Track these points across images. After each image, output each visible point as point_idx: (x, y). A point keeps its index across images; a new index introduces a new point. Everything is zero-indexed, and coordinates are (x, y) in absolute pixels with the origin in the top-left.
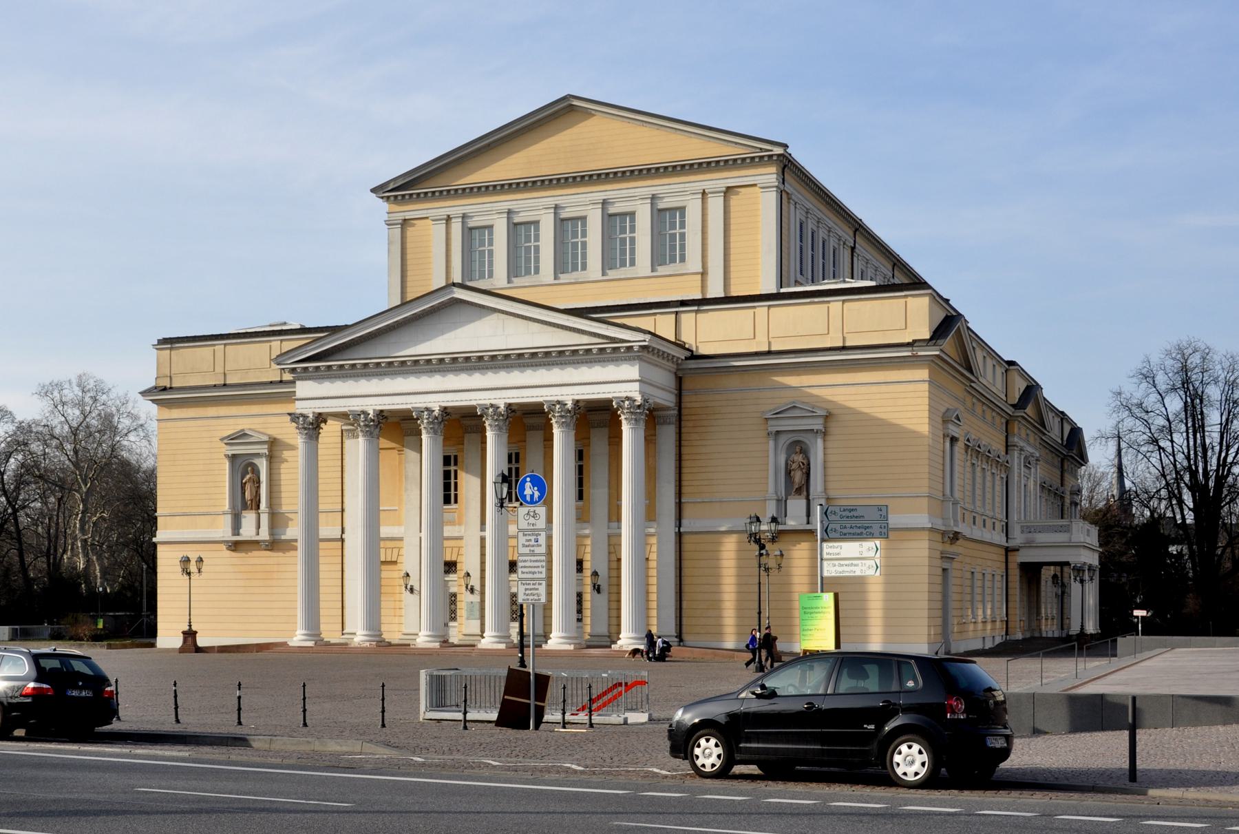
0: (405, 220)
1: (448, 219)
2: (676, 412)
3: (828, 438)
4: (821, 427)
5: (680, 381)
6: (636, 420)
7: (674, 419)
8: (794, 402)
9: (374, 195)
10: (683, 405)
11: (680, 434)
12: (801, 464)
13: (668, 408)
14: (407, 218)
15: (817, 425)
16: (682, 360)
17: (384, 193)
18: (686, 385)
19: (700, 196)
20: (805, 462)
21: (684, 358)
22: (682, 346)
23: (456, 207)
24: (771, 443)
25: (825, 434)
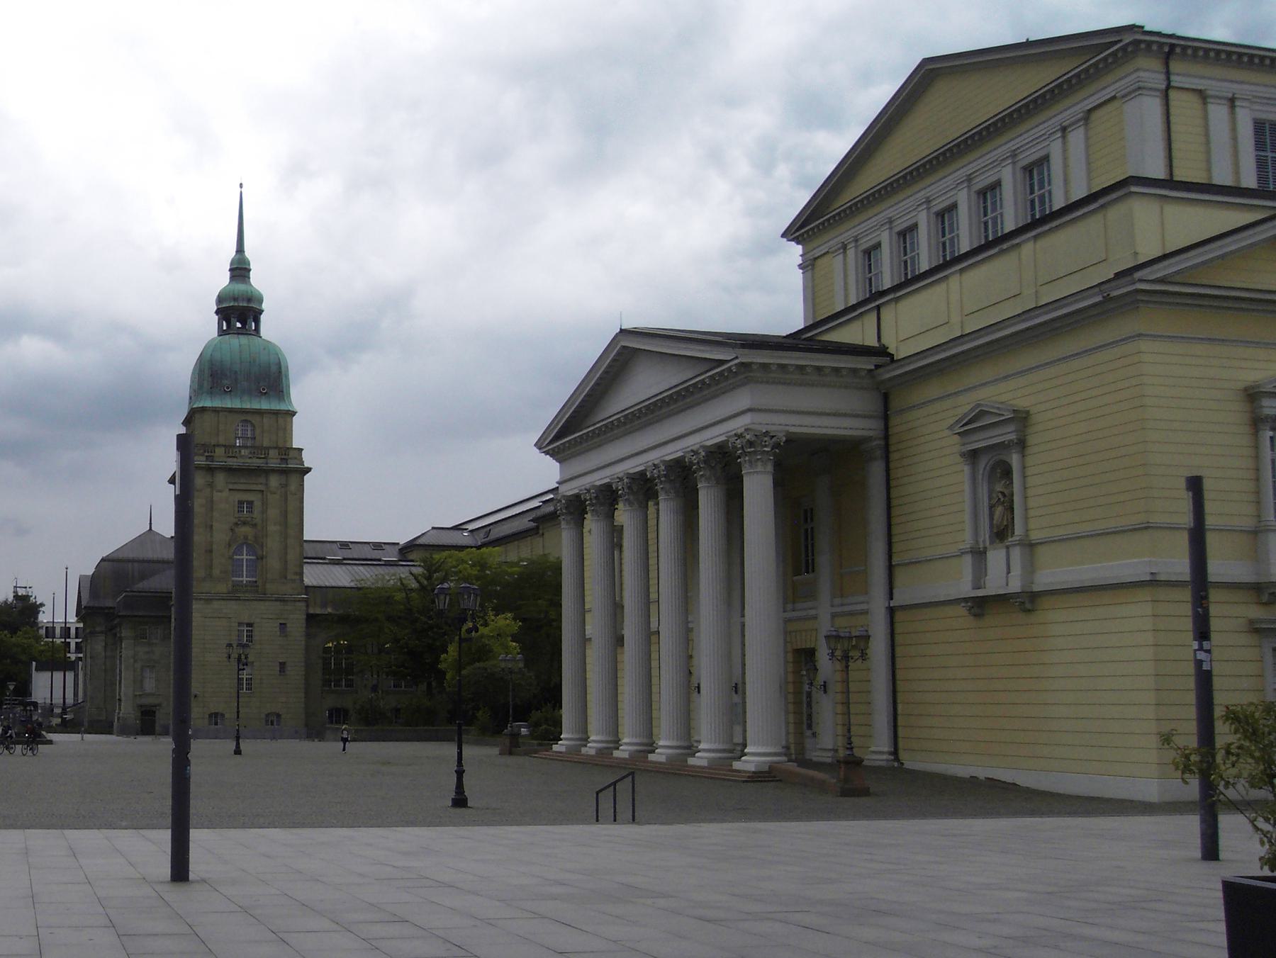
0: (816, 259)
1: (844, 247)
2: (882, 442)
3: (1028, 451)
4: (1013, 437)
5: (886, 398)
6: (750, 462)
7: (878, 453)
8: (979, 405)
9: (785, 240)
10: (891, 431)
11: (888, 470)
12: (1000, 496)
13: (869, 439)
14: (816, 256)
15: (1007, 434)
16: (870, 371)
17: (792, 235)
18: (895, 403)
19: (1059, 134)
20: (1006, 492)
21: (873, 367)
22: (882, 351)
23: (845, 232)
24: (967, 469)
25: (1022, 444)
